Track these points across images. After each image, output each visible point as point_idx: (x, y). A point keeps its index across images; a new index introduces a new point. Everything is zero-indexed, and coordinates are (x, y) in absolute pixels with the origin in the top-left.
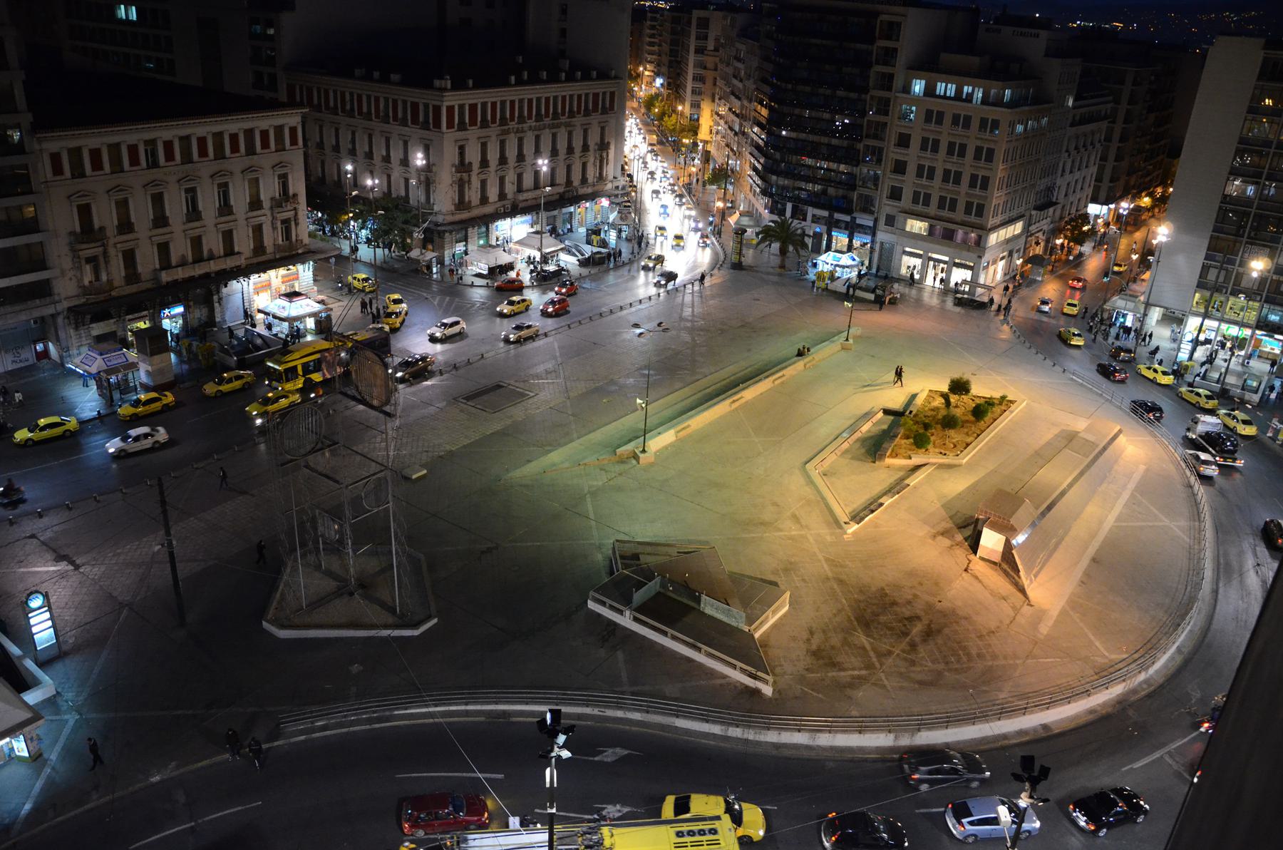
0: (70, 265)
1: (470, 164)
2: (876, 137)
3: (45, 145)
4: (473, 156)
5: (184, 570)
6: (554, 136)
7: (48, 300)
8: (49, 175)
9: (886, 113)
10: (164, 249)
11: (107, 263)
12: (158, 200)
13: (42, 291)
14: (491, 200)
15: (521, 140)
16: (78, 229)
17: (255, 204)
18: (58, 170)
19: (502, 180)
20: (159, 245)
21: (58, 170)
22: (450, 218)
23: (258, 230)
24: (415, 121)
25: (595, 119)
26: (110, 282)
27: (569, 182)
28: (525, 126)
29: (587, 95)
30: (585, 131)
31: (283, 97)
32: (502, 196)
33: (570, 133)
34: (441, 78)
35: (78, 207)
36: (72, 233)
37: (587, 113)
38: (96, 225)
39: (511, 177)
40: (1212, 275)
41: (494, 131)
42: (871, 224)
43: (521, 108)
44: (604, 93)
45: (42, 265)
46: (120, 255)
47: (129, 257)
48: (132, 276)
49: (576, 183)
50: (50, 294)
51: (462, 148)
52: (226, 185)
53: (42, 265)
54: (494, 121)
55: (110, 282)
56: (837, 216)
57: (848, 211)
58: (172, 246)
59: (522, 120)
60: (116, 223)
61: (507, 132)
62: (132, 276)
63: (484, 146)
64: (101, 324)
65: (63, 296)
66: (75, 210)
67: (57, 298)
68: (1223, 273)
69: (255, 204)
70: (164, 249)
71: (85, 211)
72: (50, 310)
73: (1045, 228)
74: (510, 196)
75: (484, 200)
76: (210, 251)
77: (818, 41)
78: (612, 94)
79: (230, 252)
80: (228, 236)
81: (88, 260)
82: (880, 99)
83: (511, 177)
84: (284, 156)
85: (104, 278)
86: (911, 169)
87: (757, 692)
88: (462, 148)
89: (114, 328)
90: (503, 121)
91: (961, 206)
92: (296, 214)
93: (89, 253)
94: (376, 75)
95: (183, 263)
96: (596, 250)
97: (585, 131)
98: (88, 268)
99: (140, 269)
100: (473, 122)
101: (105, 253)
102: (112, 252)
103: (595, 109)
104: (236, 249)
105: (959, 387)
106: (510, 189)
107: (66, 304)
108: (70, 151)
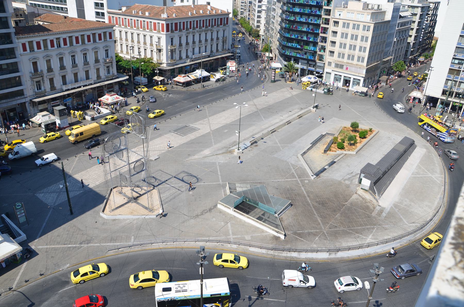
2: (324, 33)
5: (71, 195)
6: (206, 34)
7: (23, 97)
9: (328, 24)
10: (64, 77)
11: (44, 83)
12: (61, 59)
13: (21, 93)
16: (33, 71)
18: (25, 49)
19: (187, 50)
20: (62, 76)
21: (25, 49)
23: (98, 70)
24: (155, 30)
25: (221, 28)
26: (45, 90)
27: (212, 51)
28: (195, 31)
30: (218, 32)
33: (212, 33)
34: (163, 13)
35: (33, 63)
36: (31, 73)
37: (218, 26)
38: (39, 70)
39: (190, 50)
41: (184, 33)
42: (322, 65)
43: (194, 24)
44: (224, 18)
45: (20, 84)
46: (48, 80)
47: (51, 80)
52: (86, 54)
53: (20, 84)
54: (184, 29)
58: (67, 76)
59: (194, 29)
60: (46, 68)
61: (189, 33)
63: (180, 38)
64: (42, 105)
65: (28, 95)
67: (26, 96)
69: (97, 61)
70: (64, 77)
71: (35, 64)
72: (23, 101)
73: (387, 66)
74: (190, 56)
76: (81, 78)
79: (88, 78)
80: (87, 72)
82: (326, 19)
83: (190, 50)
85: (43, 88)
87: (279, 237)
89: (47, 107)
90: (187, 29)
92: (112, 64)
95: (71, 83)
97: (218, 32)
99: (55, 85)
100: (176, 29)
101: (43, 79)
103: (221, 24)
104: (90, 77)
105: (355, 127)
108: (29, 42)
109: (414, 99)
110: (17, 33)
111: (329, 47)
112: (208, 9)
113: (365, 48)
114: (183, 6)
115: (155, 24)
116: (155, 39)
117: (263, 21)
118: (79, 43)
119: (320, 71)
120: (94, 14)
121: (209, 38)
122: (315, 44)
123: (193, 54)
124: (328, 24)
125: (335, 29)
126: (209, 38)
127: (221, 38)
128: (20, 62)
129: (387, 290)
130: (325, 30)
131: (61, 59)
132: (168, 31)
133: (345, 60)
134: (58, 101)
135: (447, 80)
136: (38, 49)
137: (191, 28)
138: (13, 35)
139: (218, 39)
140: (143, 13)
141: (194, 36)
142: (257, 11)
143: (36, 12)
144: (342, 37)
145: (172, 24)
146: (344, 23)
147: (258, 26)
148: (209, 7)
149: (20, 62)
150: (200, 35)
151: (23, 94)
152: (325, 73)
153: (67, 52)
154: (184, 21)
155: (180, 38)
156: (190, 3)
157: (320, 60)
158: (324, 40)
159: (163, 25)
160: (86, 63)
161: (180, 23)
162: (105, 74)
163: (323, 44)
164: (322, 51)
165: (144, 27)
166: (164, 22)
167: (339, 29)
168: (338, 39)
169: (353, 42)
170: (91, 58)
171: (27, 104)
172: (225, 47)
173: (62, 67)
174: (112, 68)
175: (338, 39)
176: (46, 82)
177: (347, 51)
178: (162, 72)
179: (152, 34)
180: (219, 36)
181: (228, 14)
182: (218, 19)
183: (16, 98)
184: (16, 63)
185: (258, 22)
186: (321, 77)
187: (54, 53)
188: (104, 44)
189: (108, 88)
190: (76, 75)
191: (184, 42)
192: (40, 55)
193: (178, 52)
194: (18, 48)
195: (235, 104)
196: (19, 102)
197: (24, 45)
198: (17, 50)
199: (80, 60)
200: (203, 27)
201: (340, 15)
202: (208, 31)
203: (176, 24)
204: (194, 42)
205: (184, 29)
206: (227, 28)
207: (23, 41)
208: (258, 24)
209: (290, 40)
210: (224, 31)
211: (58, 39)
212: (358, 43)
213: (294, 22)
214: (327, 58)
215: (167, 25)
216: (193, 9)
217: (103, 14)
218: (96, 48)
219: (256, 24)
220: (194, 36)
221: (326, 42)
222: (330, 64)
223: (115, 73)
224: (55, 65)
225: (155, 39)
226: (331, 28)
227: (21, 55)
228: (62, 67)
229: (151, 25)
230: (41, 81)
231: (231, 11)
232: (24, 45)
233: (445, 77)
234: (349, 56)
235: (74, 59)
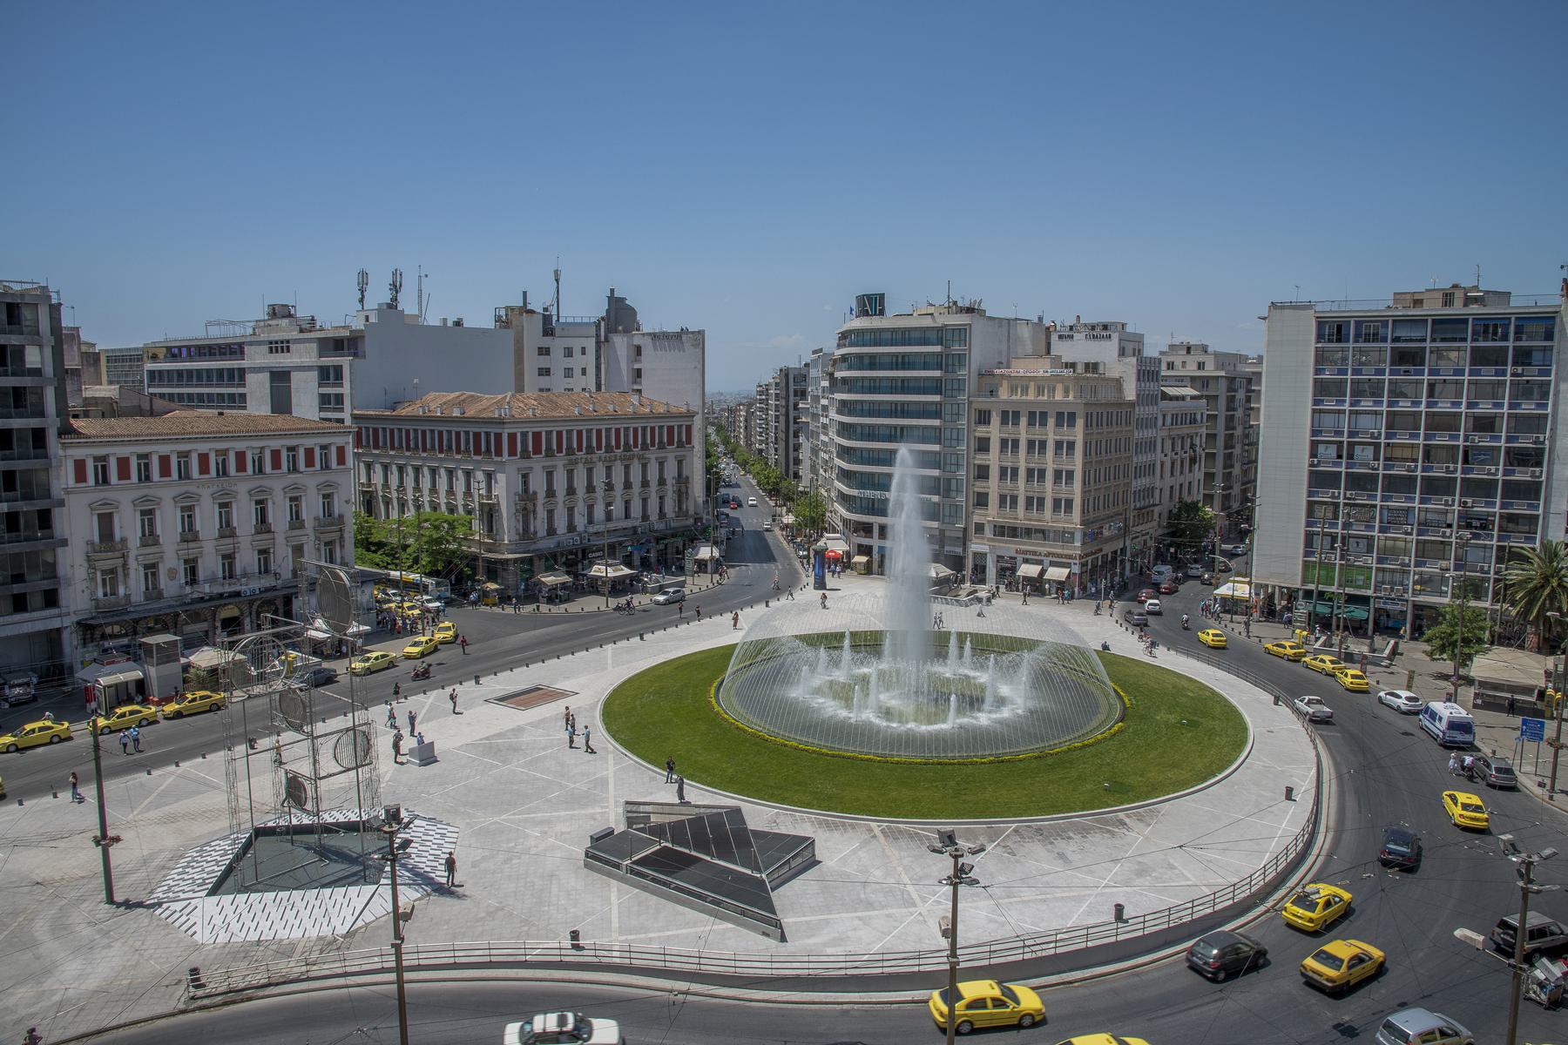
0: (85, 576)
1: (535, 493)
3: (70, 452)
4: (538, 484)
8: (72, 482)
11: (126, 575)
15: (590, 471)
16: (96, 539)
21: (80, 476)
24: (478, 451)
26: (127, 596)
28: (595, 457)
29: (661, 428)
36: (90, 543)
37: (662, 446)
38: (117, 537)
41: (560, 462)
44: (680, 427)
47: (151, 569)
48: (153, 593)
51: (525, 476)
54: (560, 450)
55: (127, 596)
59: (590, 450)
62: (153, 593)
63: (550, 474)
65: (72, 609)
66: (95, 518)
67: (64, 610)
71: (106, 522)
72: (56, 624)
75: (551, 531)
85: (121, 590)
88: (525, 476)
92: (342, 537)
93: (108, 565)
100: (537, 450)
101: (125, 566)
102: (132, 564)
103: (671, 442)
106: (580, 521)
107: (75, 619)
115: (477, 436)
129: (1521, 884)
132: (512, 452)
136: (120, 478)
137: (580, 449)
139: (662, 482)
141: (590, 471)
145: (524, 435)
155: (550, 474)
161: (549, 433)
170: (279, 516)
171: (66, 635)
174: (342, 547)
176: (132, 573)
182: (661, 428)
188: (322, 478)
190: (229, 558)
193: (542, 514)
194: (62, 473)
197: (80, 466)
198: (58, 478)
200: (618, 447)
202: (631, 458)
203: (537, 436)
205: (560, 450)
211: (185, 455)
227: (67, 491)
230: (120, 570)
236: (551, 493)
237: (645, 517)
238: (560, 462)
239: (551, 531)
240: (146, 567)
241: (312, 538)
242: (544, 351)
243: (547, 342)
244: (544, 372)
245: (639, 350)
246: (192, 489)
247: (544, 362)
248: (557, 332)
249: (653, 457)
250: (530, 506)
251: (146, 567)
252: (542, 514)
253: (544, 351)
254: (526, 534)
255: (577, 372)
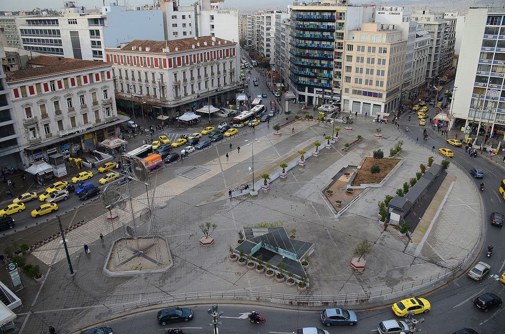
2: (338, 58)
4: (180, 77)
5: (71, 251)
8: (14, 98)
9: (342, 48)
11: (38, 130)
12: (56, 103)
13: (14, 142)
14: (188, 94)
17: (95, 103)
18: (17, 95)
21: (17, 95)
22: (173, 103)
23: (97, 112)
24: (157, 66)
26: (40, 137)
31: (104, 59)
32: (193, 92)
37: (224, 58)
39: (196, 85)
40: (475, 103)
41: (188, 68)
43: (198, 57)
47: (46, 126)
49: (222, 85)
50: (17, 144)
54: (187, 63)
55: (40, 137)
56: (325, 90)
57: (330, 88)
65: (22, 144)
68: (480, 102)
69: (95, 103)
72: (17, 150)
75: (186, 95)
77: (313, 23)
78: (234, 49)
81: (31, 130)
82: (339, 43)
83: (196, 85)
84: (106, 84)
85: (38, 136)
86: (354, 69)
91: (374, 83)
94: (140, 49)
96: (231, 110)
98: (31, 132)
100: (179, 64)
102: (40, 125)
103: (227, 56)
104: (89, 121)
106: (196, 90)
109: (440, 121)
110: (8, 79)
111: (345, 74)
112: (212, 41)
113: (383, 71)
114: (185, 39)
115: (156, 59)
116: (157, 76)
117: (272, 50)
118: (75, 85)
119: (337, 98)
120: (91, 54)
121: (215, 71)
122: (329, 69)
123: (199, 89)
124: (342, 48)
125: (349, 53)
126: (215, 71)
127: (228, 71)
128: (12, 109)
130: (339, 55)
131: (56, 103)
132: (170, 66)
133: (363, 85)
134: (55, 148)
135: (473, 100)
136: (31, 94)
138: (4, 81)
139: (225, 71)
140: (144, 50)
141: (199, 69)
142: (265, 40)
143: (29, 55)
144: (358, 61)
146: (359, 47)
147: (268, 56)
148: (213, 39)
149: (12, 109)
150: (205, 68)
151: (16, 143)
152: (342, 101)
153: (62, 95)
154: (187, 55)
156: (194, 35)
157: (336, 87)
158: (339, 65)
159: (165, 60)
160: (84, 106)
162: (104, 116)
163: (338, 70)
164: (338, 77)
165: (145, 63)
166: (165, 57)
167: (354, 53)
168: (354, 64)
169: (370, 66)
170: (88, 100)
171: (21, 154)
172: (233, 81)
173: (58, 112)
175: (354, 64)
177: (364, 76)
178: (166, 111)
179: (153, 71)
180: (226, 69)
181: (235, 44)
183: (9, 148)
184: (8, 111)
185: (268, 50)
186: (339, 105)
187: (48, 97)
189: (109, 132)
191: (188, 77)
192: (33, 101)
193: (182, 88)
194: (10, 96)
195: (247, 141)
196: (12, 152)
197: (16, 91)
199: (76, 102)
201: (353, 38)
204: (199, 77)
205: (187, 63)
206: (234, 59)
207: (15, 86)
208: (268, 53)
209: (303, 67)
210: (231, 63)
212: (376, 67)
213: (306, 48)
214: (344, 85)
215: (170, 60)
216: (197, 41)
217: (100, 53)
218: (93, 89)
219: (265, 53)
220: (199, 69)
221: (341, 68)
222: (347, 90)
223: (116, 115)
224: (50, 109)
225: (157, 76)
226: (346, 52)
228: (58, 112)
229: (152, 61)
230: (36, 128)
231: (237, 40)
232: (16, 91)
233: (471, 97)
234: (367, 81)
235: (70, 102)
236: (185, 80)
237: (219, 85)
238: (188, 68)
239: (186, 95)
240: (45, 125)
241: (101, 107)
242: (174, 17)
243: (175, 13)
244: (175, 25)
245: (212, 18)
246: (57, 95)
247: (174, 21)
248: (179, 9)
249: (221, 62)
250: (178, 86)
251: (45, 125)
252: (182, 88)
253: (174, 17)
254: (177, 97)
255: (187, 25)
